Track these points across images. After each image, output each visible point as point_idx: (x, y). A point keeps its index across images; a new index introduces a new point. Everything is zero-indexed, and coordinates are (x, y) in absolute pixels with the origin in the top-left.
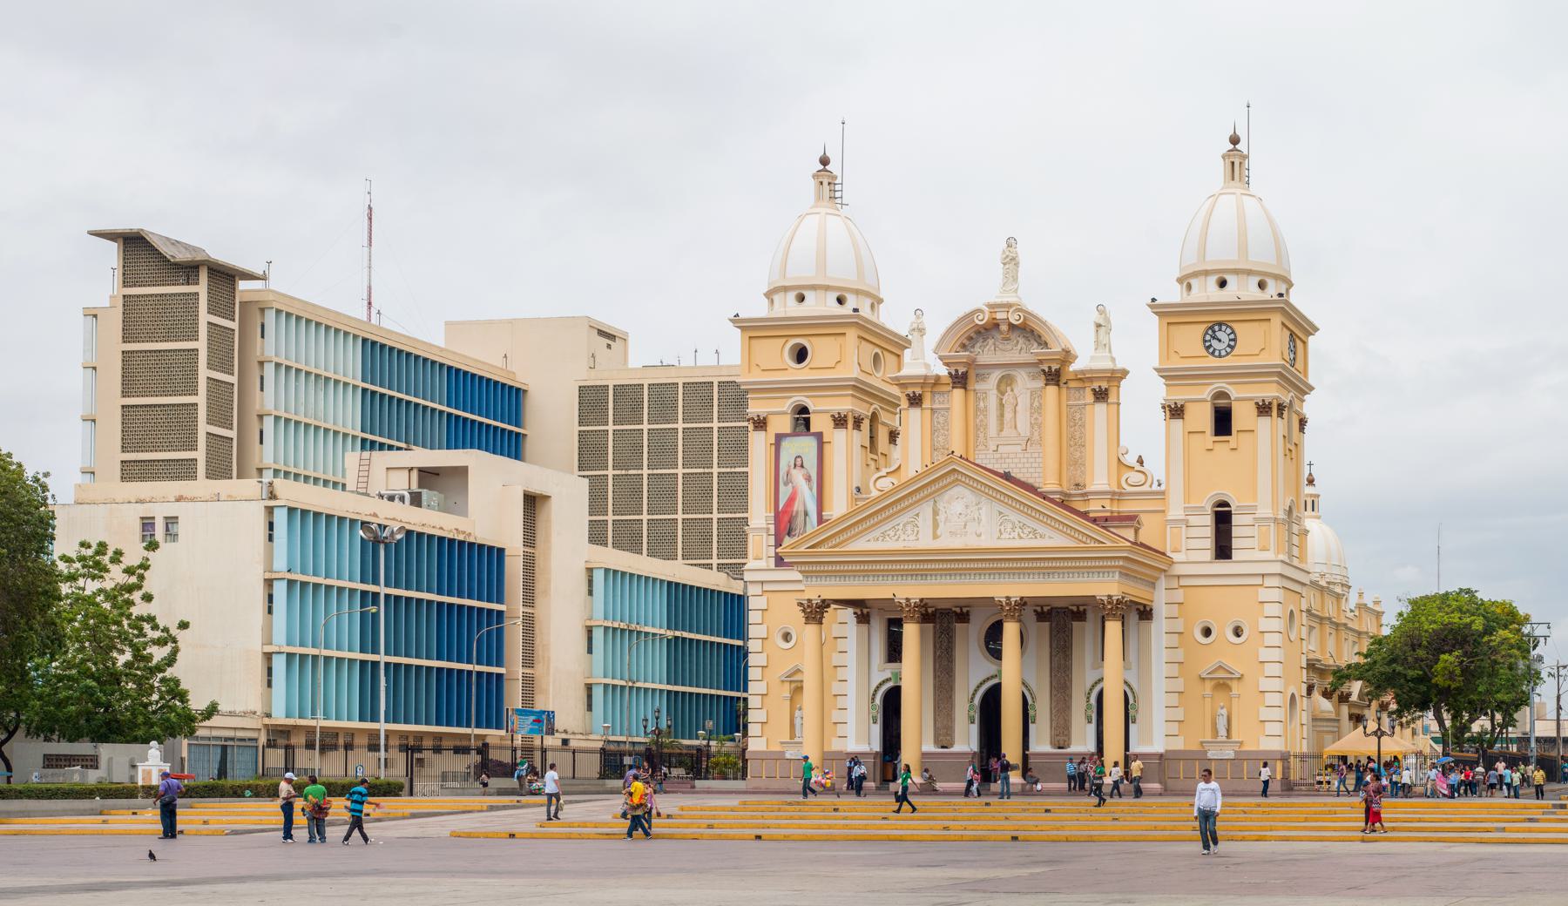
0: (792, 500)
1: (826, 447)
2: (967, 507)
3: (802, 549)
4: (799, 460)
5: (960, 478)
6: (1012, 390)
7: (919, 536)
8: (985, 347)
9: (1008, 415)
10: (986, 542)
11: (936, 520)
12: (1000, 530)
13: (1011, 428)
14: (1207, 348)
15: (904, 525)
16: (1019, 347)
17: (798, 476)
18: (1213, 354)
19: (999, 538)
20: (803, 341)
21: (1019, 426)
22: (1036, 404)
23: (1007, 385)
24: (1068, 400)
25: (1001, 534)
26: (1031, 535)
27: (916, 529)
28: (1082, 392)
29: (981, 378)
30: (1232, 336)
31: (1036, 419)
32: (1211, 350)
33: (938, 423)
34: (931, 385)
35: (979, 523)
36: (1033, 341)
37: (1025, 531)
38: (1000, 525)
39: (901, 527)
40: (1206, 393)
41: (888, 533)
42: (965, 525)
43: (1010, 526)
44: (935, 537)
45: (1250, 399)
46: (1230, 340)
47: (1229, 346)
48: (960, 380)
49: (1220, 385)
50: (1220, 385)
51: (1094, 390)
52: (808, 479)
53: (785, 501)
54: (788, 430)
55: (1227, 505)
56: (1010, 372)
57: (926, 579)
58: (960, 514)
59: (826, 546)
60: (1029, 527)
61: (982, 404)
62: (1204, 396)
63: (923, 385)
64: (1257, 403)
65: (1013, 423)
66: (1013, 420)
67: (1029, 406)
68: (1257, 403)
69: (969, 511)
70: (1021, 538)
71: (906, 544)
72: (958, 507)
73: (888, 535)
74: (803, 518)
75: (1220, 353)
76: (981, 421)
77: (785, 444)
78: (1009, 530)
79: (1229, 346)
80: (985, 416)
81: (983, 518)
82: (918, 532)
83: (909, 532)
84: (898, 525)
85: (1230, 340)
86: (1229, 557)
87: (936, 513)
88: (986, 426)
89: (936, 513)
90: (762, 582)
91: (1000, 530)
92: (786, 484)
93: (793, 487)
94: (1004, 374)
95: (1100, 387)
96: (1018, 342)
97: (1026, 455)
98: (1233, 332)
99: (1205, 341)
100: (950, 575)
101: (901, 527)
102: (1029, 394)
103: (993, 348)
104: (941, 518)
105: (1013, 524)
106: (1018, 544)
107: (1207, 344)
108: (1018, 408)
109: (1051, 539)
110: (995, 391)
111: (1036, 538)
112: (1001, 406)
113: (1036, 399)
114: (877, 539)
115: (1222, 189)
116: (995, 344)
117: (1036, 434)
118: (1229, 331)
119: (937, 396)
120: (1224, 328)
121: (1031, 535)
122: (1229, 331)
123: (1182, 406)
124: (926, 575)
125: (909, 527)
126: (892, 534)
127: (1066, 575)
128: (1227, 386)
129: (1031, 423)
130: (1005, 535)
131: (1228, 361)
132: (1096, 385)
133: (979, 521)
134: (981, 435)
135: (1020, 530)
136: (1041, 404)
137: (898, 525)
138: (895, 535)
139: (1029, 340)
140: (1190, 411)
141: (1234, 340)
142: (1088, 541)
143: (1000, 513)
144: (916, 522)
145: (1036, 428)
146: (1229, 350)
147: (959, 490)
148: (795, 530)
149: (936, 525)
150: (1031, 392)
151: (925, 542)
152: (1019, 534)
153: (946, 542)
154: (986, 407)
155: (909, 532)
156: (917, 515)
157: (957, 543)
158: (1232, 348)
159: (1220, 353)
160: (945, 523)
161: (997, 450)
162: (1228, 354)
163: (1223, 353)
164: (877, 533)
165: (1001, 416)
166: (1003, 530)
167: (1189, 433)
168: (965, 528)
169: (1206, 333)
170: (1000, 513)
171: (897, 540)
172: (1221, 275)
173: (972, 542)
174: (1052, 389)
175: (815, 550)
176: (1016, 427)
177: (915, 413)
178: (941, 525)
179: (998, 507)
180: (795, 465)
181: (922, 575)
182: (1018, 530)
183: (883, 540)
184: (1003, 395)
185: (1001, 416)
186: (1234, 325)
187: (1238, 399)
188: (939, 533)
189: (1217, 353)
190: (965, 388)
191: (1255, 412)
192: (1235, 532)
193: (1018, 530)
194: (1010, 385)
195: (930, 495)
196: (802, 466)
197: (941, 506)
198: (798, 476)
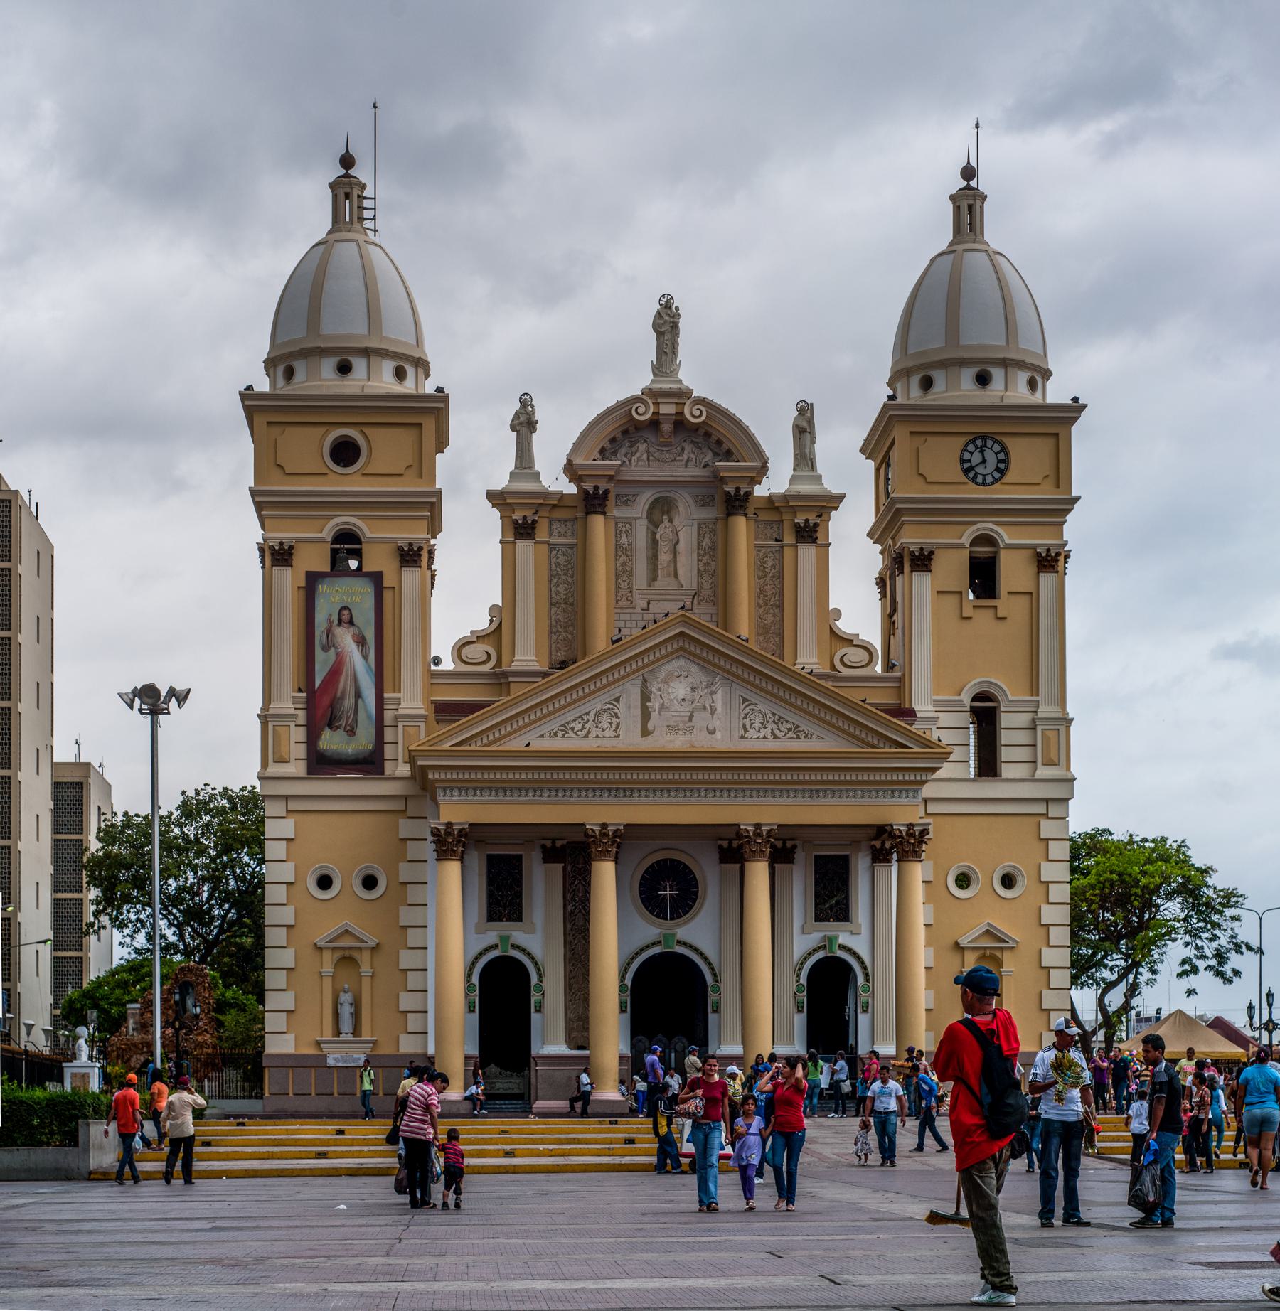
0: (335, 672)
1: (387, 595)
2: (693, 689)
3: (446, 746)
4: (346, 612)
5: (687, 646)
6: (671, 521)
7: (621, 730)
9: (664, 558)
10: (721, 742)
11: (647, 707)
12: (744, 726)
13: (669, 576)
14: (966, 471)
15: (597, 715)
16: (685, 457)
17: (346, 639)
18: (974, 480)
19: (742, 737)
20: (353, 433)
21: (681, 572)
22: (707, 542)
23: (663, 513)
24: (756, 539)
25: (746, 731)
26: (790, 735)
27: (614, 720)
28: (775, 528)
29: (626, 501)
30: (1001, 456)
31: (707, 564)
32: (971, 475)
33: (558, 564)
34: (549, 508)
35: (712, 714)
36: (705, 450)
37: (782, 729)
39: (592, 715)
41: (573, 725)
42: (691, 717)
44: (645, 732)
45: (1034, 548)
47: (997, 469)
48: (593, 502)
49: (987, 525)
50: (987, 525)
51: (797, 526)
52: (361, 642)
53: (324, 674)
54: (321, 563)
56: (668, 494)
57: (631, 796)
58: (683, 700)
59: (479, 743)
60: (787, 721)
61: (624, 540)
63: (538, 508)
65: (672, 569)
66: (672, 565)
67: (695, 544)
69: (697, 696)
70: (776, 737)
71: (599, 742)
72: (679, 690)
73: (573, 729)
74: (352, 700)
75: (984, 479)
76: (624, 564)
77: (323, 588)
78: (757, 725)
79: (997, 469)
80: (630, 557)
81: (719, 708)
82: (618, 725)
83: (605, 725)
84: (588, 713)
85: (999, 461)
87: (645, 697)
88: (631, 573)
89: (645, 697)
90: (287, 798)
91: (744, 726)
92: (325, 648)
93: (338, 654)
94: (658, 495)
95: (807, 521)
98: (1004, 449)
99: (962, 461)
100: (669, 791)
101: (592, 715)
104: (654, 704)
105: (764, 716)
106: (771, 745)
107: (966, 465)
108: (681, 547)
109: (821, 742)
110: (645, 522)
111: (798, 738)
112: (654, 543)
113: (707, 535)
114: (555, 735)
115: (951, 244)
117: (707, 586)
118: (997, 448)
119: (556, 525)
120: (989, 443)
124: (632, 790)
125: (605, 718)
127: (844, 792)
129: (699, 570)
130: (751, 734)
131: (999, 492)
132: (800, 519)
133: (713, 713)
134: (624, 586)
135: (775, 727)
137: (588, 713)
138: (583, 728)
139: (700, 448)
140: (937, 563)
141: (1006, 461)
142: (881, 745)
143: (745, 700)
144: (616, 711)
145: (706, 577)
146: (997, 475)
147: (676, 665)
148: (340, 718)
149: (646, 715)
151: (631, 739)
153: (661, 740)
154: (630, 544)
155: (605, 725)
156: (617, 700)
157: (678, 742)
158: (1002, 472)
159: (984, 479)
160: (660, 712)
161: (648, 609)
162: (995, 481)
163: (989, 479)
164: (554, 725)
165: (654, 559)
166: (748, 726)
168: (690, 720)
169: (965, 450)
170: (745, 700)
171: (586, 736)
172: (983, 367)
173: (702, 742)
174: (741, 525)
175: (467, 748)
176: (676, 576)
177: (525, 549)
178: (654, 715)
179: (740, 692)
180: (340, 621)
181: (625, 790)
182: (771, 726)
183: (563, 736)
185: (654, 559)
187: (1010, 547)
188: (650, 726)
189: (980, 479)
190: (604, 513)
193: (771, 726)
194: (668, 512)
195: (636, 671)
196: (351, 623)
198: (346, 639)
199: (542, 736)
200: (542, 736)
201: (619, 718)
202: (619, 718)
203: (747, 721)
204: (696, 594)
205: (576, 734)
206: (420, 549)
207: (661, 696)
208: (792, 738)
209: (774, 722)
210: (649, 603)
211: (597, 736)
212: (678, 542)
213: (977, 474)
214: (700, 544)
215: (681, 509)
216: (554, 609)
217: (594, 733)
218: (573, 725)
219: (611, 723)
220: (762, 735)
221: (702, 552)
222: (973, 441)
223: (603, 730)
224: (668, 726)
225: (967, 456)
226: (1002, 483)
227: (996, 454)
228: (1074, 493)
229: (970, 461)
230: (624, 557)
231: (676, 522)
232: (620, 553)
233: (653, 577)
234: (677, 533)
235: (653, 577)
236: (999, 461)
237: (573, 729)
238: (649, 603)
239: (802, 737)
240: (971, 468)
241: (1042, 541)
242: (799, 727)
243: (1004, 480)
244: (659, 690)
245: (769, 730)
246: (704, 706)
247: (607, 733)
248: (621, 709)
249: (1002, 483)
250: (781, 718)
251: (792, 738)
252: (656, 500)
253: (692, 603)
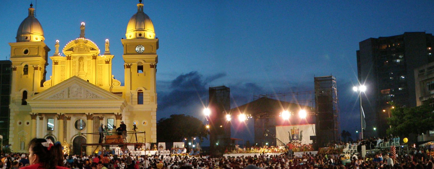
2: (78, 89)
6: (83, 61)
7: (64, 97)
8: (76, 50)
9: (81, 67)
15: (60, 94)
16: (85, 50)
19: (86, 98)
26: (96, 97)
27: (63, 95)
31: (89, 68)
33: (62, 69)
38: (87, 94)
41: (56, 96)
42: (77, 94)
43: (90, 94)
44: (69, 97)
55: (142, 91)
58: (76, 91)
60: (95, 95)
78: (89, 95)
81: (82, 92)
82: (64, 96)
83: (61, 96)
84: (58, 94)
87: (69, 91)
88: (75, 70)
89: (69, 91)
96: (85, 49)
97: (86, 77)
101: (59, 94)
102: (87, 62)
103: (78, 50)
110: (78, 61)
112: (80, 65)
113: (89, 63)
114: (52, 98)
116: (78, 49)
119: (62, 62)
120: (141, 46)
121: (96, 97)
125: (61, 95)
126: (56, 96)
129: (88, 69)
130: (88, 97)
133: (81, 93)
134: (74, 72)
135: (92, 95)
136: (90, 64)
144: (63, 93)
149: (69, 94)
150: (88, 62)
152: (92, 97)
156: (64, 91)
170: (87, 91)
171: (58, 98)
176: (83, 70)
178: (70, 94)
184: (80, 62)
185: (80, 67)
188: (70, 96)
191: (149, 66)
194: (82, 59)
197: (70, 89)
199: (50, 98)
200: (50, 98)
201: (64, 94)
202: (64, 94)
203: (87, 95)
204: (87, 73)
205: (56, 97)
206: (38, 67)
207: (72, 91)
208: (96, 98)
209: (93, 95)
210: (78, 75)
211: (60, 98)
212: (84, 64)
214: (88, 65)
215: (85, 59)
216: (61, 76)
217: (59, 97)
218: (56, 96)
219: (62, 95)
220: (90, 97)
221: (88, 66)
223: (61, 97)
224: (73, 96)
230: (74, 67)
231: (84, 61)
232: (73, 66)
233: (79, 70)
234: (84, 63)
235: (79, 70)
237: (55, 97)
238: (78, 75)
239: (98, 97)
242: (97, 96)
244: (71, 89)
245: (91, 96)
246: (79, 92)
247: (62, 97)
248: (64, 93)
250: (94, 94)
251: (96, 98)
252: (80, 57)
253: (86, 75)
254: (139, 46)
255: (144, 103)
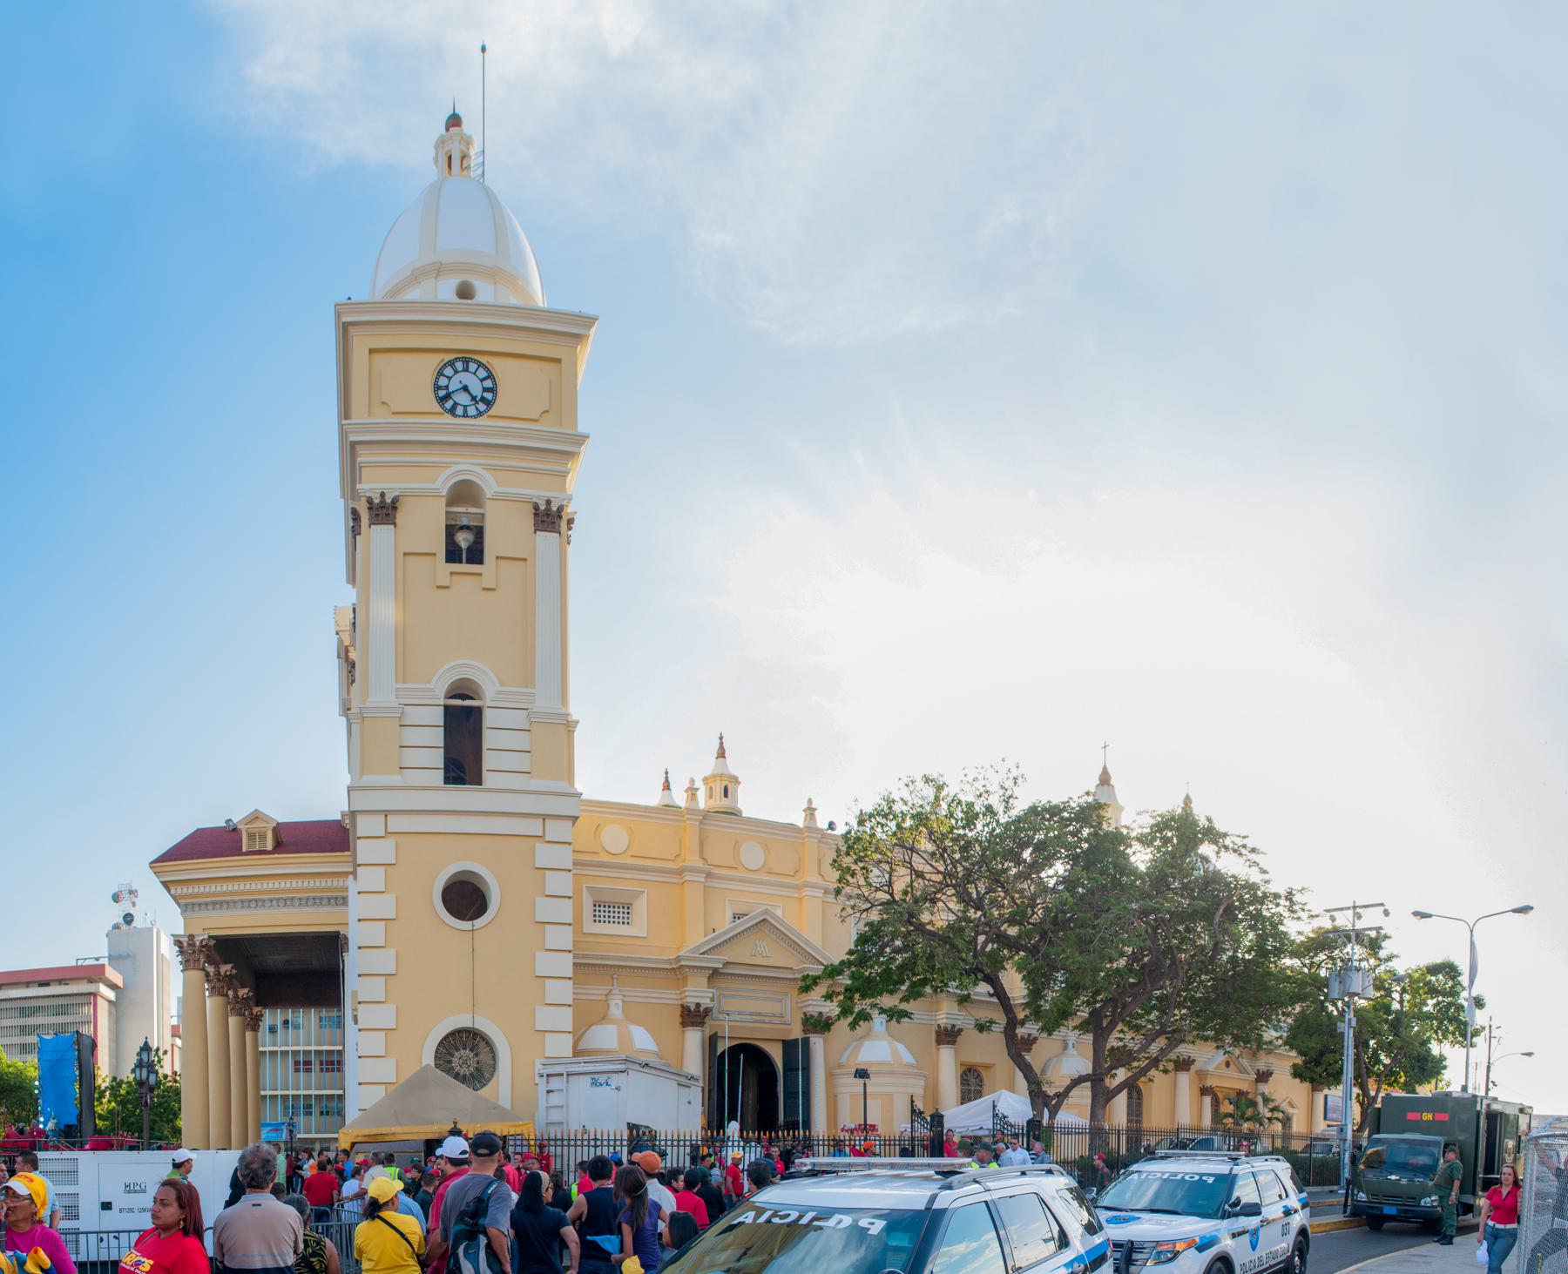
14: (442, 400)
18: (452, 411)
30: (488, 384)
32: (449, 405)
40: (442, 483)
46: (485, 390)
62: (437, 485)
64: (536, 507)
68: (536, 507)
75: (465, 411)
86: (478, 780)
98: (490, 376)
99: (437, 388)
107: (442, 393)
118: (482, 373)
120: (473, 367)
122: (482, 373)
123: (395, 500)
128: (485, 474)
141: (493, 390)
158: (489, 403)
159: (465, 411)
162: (480, 414)
167: (405, 554)
169: (440, 373)
186: (497, 365)
192: (489, 739)
213: (456, 404)
222: (451, 363)
225: (443, 382)
226: (489, 416)
227: (482, 380)
228: (581, 429)
229: (447, 387)
236: (485, 390)
240: (448, 396)
241: (539, 492)
243: (490, 413)
249: (489, 416)
254: (459, 366)
255: (489, 779)
